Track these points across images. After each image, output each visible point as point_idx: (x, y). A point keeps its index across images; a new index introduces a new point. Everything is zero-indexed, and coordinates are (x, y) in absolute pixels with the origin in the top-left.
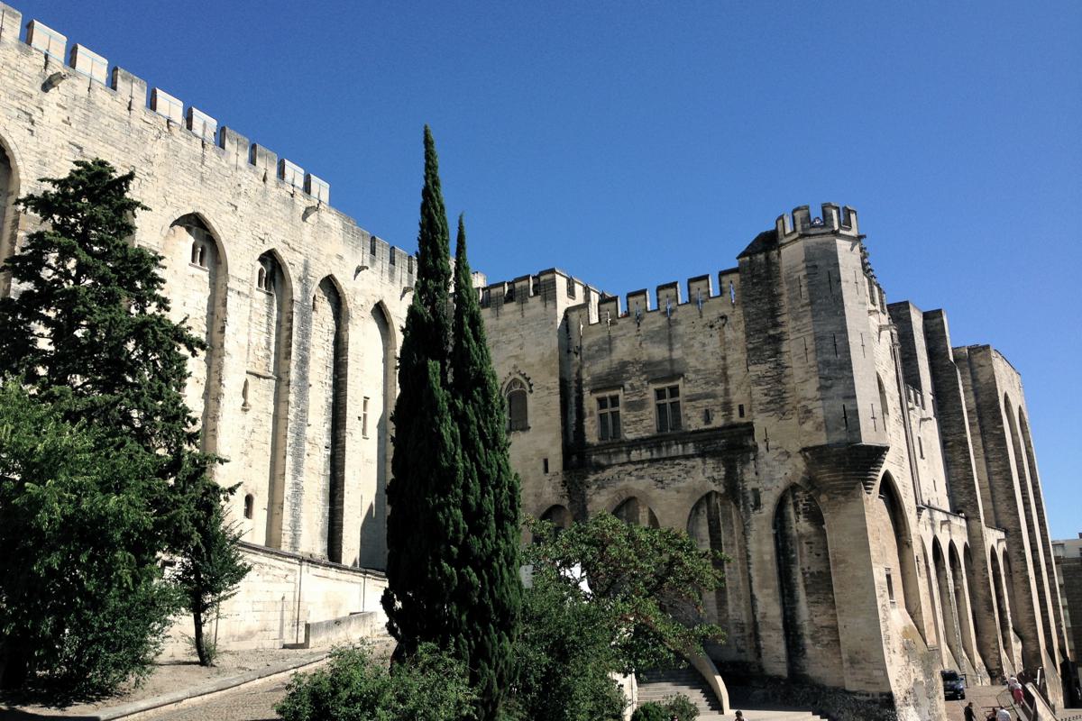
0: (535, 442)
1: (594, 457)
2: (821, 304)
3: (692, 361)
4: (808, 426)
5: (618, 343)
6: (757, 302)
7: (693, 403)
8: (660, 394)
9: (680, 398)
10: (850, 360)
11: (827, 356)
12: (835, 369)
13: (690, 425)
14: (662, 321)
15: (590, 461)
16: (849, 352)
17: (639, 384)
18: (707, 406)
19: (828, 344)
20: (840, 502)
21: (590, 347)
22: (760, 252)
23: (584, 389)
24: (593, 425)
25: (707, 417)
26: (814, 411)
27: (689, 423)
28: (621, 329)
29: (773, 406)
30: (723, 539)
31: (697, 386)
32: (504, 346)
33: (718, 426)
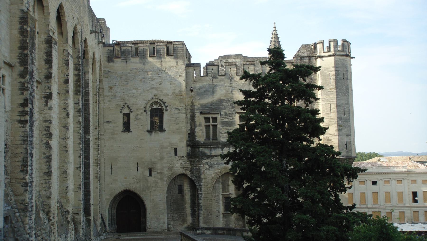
0: (169, 138)
1: (201, 149)
2: (340, 89)
5: (218, 89)
10: (350, 118)
11: (341, 115)
12: (344, 122)
15: (199, 151)
16: (349, 114)
17: (230, 112)
19: (341, 109)
21: (200, 88)
22: (307, 57)
23: (196, 111)
24: (201, 132)
26: (333, 140)
28: (220, 81)
32: (148, 81)
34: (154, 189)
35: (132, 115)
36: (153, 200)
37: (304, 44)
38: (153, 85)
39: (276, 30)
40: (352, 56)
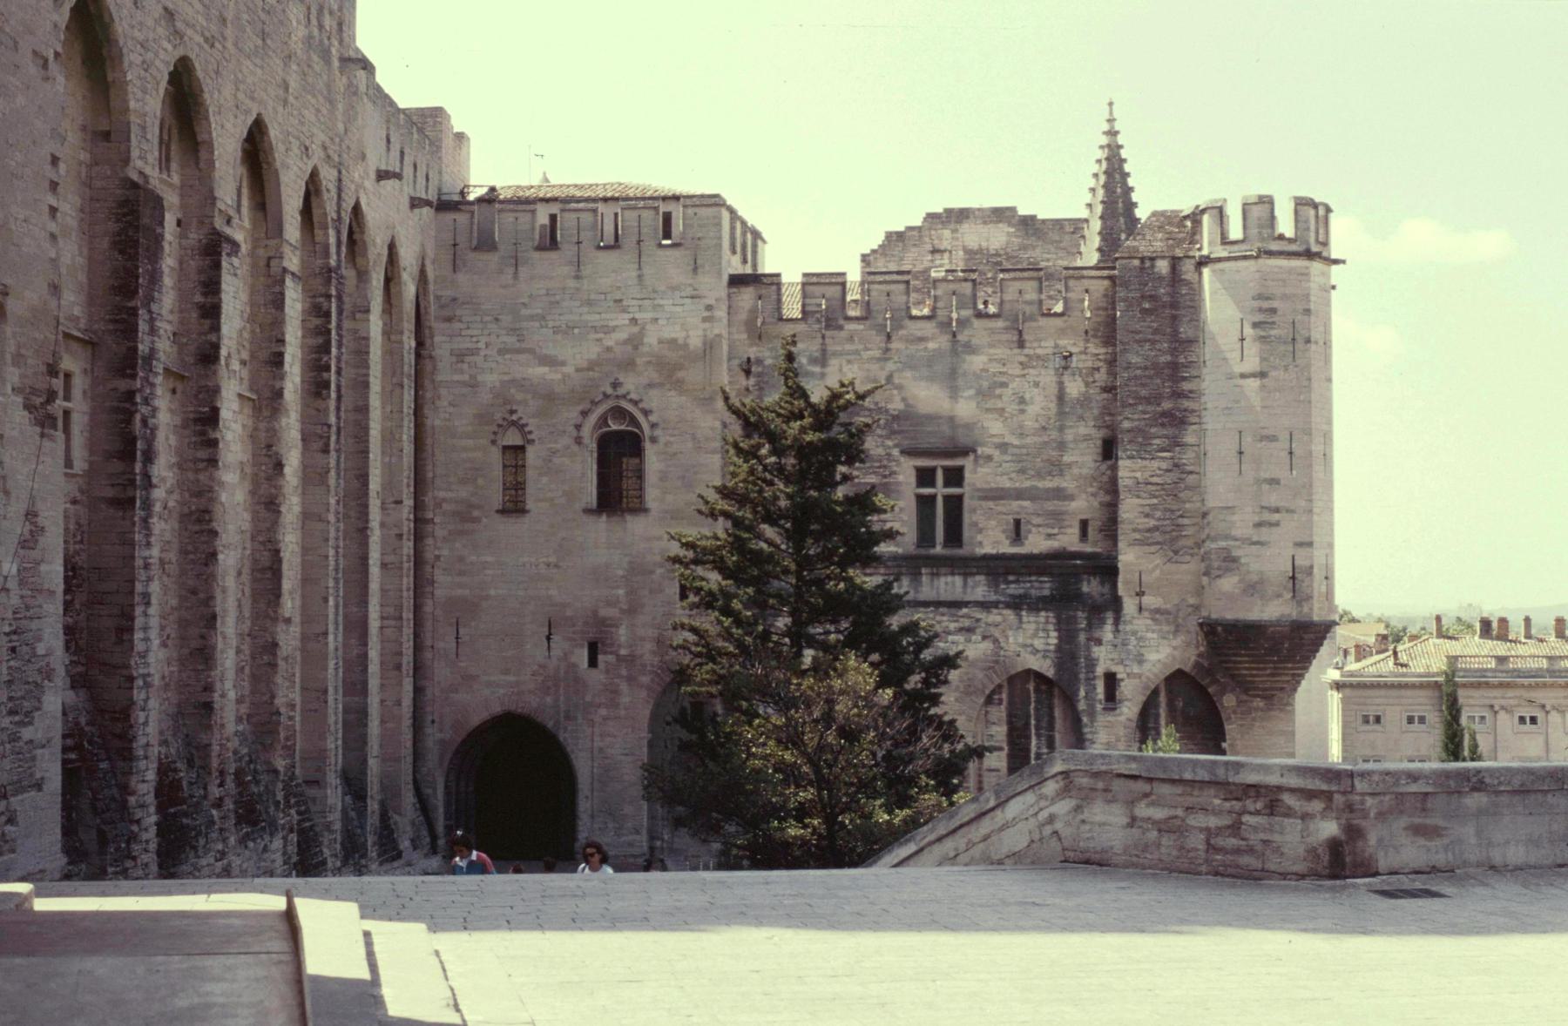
3: (995, 427)
4: (1228, 583)
6: (1147, 346)
7: (991, 504)
8: (925, 477)
9: (966, 490)
13: (980, 543)
14: (938, 343)
17: (880, 451)
18: (1018, 513)
20: (1257, 709)
22: (1163, 258)
25: (1017, 531)
26: (1243, 561)
27: (979, 538)
28: (851, 339)
29: (1157, 536)
30: (1033, 749)
31: (1002, 474)
33: (1036, 551)
34: (603, 712)
35: (532, 454)
36: (601, 750)
37: (1160, 208)
38: (609, 349)
39: (1117, 128)
40: (1333, 256)
